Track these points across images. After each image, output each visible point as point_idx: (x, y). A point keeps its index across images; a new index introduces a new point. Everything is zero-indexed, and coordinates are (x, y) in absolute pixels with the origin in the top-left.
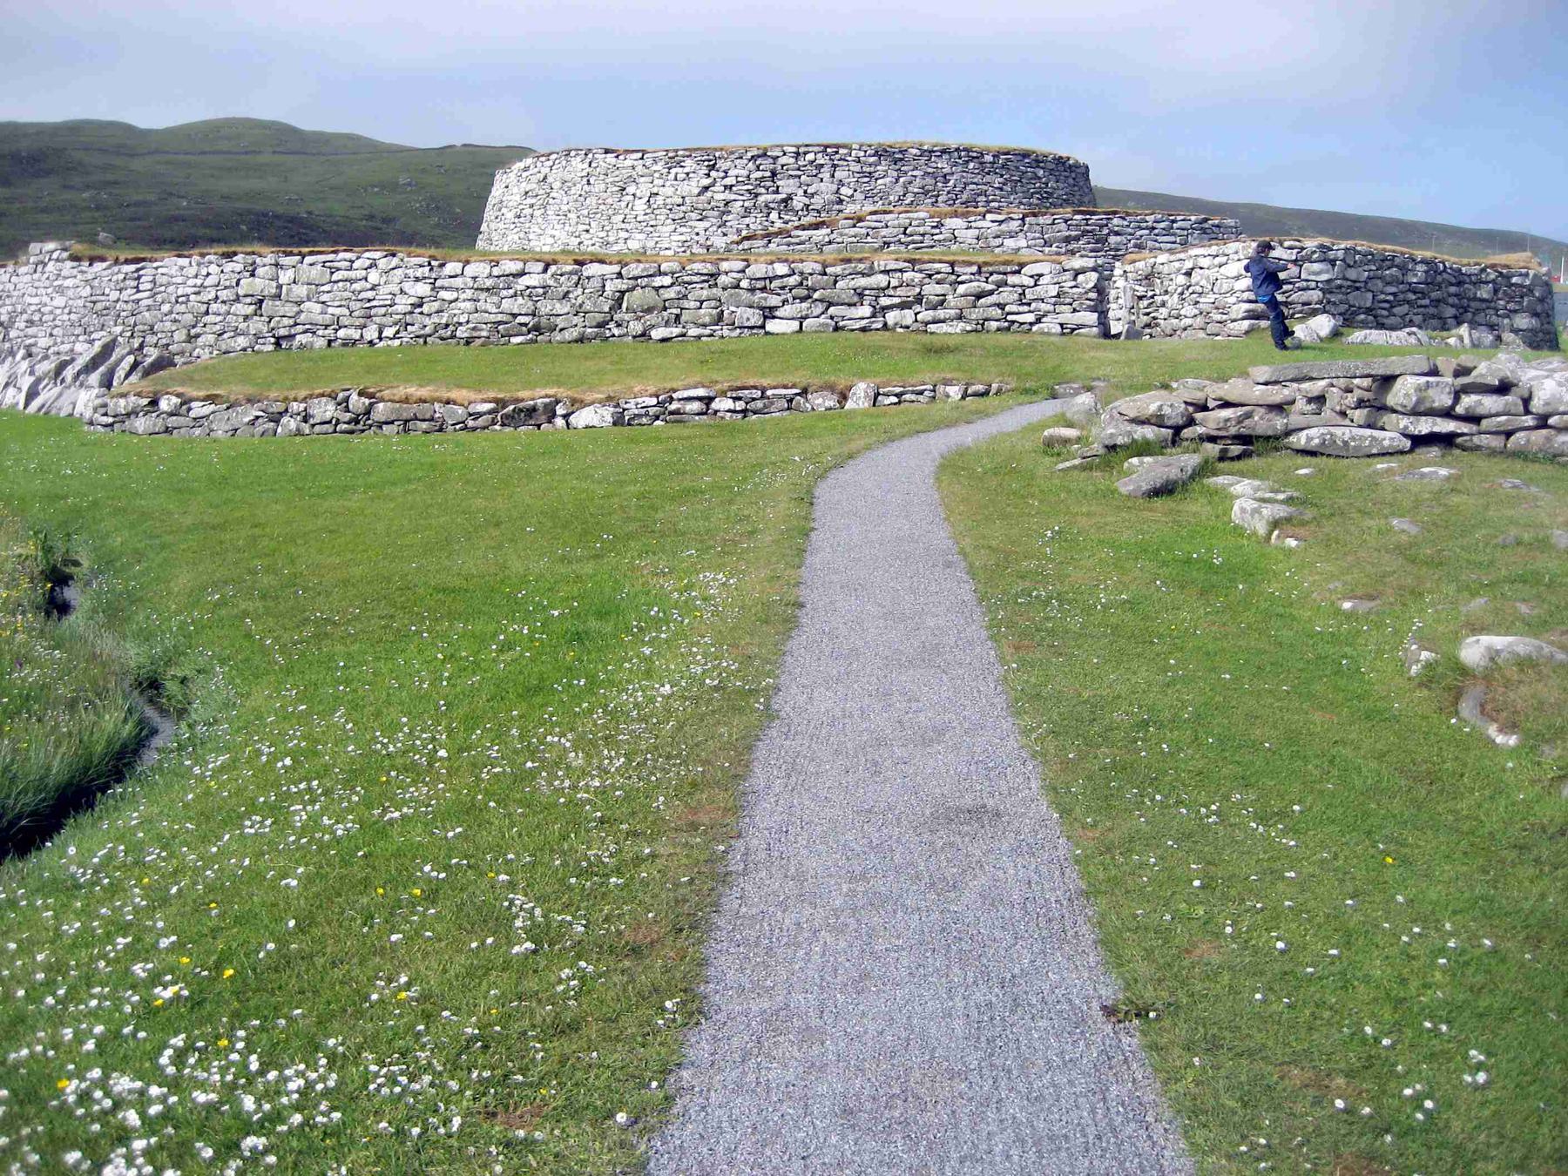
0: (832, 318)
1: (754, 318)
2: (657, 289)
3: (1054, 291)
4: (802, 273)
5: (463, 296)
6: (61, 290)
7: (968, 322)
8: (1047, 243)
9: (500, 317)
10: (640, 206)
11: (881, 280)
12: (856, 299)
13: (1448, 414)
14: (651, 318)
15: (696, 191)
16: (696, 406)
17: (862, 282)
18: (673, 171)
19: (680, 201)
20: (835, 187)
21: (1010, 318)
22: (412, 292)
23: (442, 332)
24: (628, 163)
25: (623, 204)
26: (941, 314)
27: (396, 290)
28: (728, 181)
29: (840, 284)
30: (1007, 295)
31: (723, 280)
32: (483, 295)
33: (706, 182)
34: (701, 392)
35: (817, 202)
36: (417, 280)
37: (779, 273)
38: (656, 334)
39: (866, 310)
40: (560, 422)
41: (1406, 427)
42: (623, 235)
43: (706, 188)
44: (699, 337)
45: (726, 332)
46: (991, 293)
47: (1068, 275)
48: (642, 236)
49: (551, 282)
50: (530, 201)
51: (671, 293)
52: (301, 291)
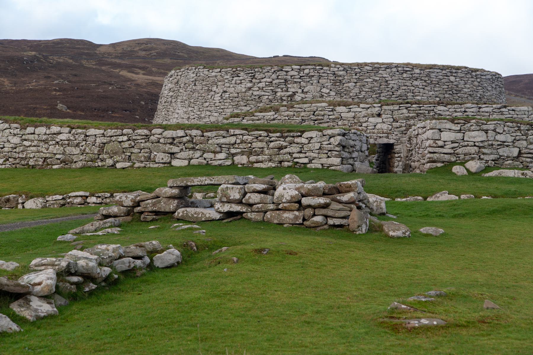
0: (205, 159)
1: (167, 158)
2: (120, 142)
3: (317, 146)
4: (190, 136)
5: (33, 144)
7: (274, 162)
8: (395, 120)
9: (48, 155)
10: (217, 98)
11: (232, 140)
12: (218, 149)
13: (239, 202)
14: (116, 158)
15: (244, 90)
16: (79, 200)
17: (222, 141)
18: (235, 78)
19: (236, 95)
20: (319, 89)
21: (295, 160)
22: (12, 141)
23: (23, 162)
24: (214, 74)
25: (210, 96)
26: (260, 158)
27: (5, 140)
28: (260, 85)
29: (210, 142)
30: (294, 149)
31: (152, 138)
32: (41, 144)
33: (249, 85)
34: (81, 193)
35: (309, 96)
36: (15, 135)
37: (179, 135)
38: (119, 165)
40: (20, 206)
41: (219, 208)
42: (208, 113)
43: (250, 89)
44: (139, 168)
45: (152, 166)
46: (286, 147)
47: (325, 138)
48: (216, 114)
49: (72, 138)
50: (171, 94)
51: (126, 145)
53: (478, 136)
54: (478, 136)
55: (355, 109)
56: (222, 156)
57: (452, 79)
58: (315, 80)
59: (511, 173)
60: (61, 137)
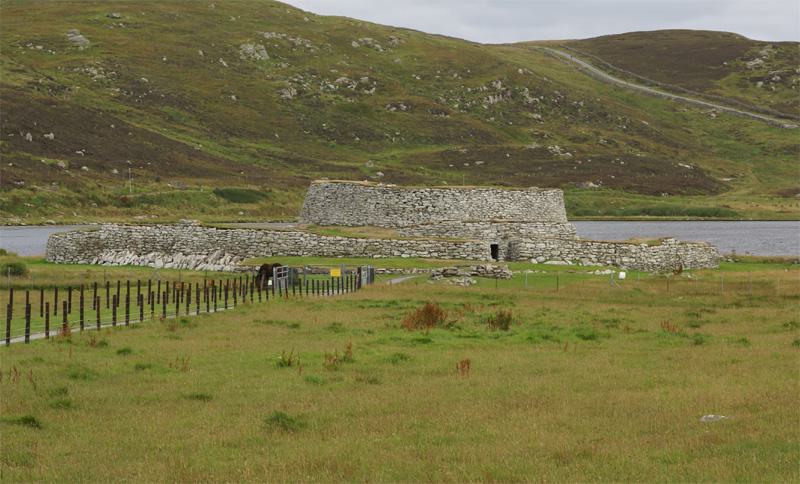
6: (196, 235)
10: (372, 207)
39: (426, 253)
52: (280, 241)
53: (542, 246)
54: (542, 246)
55: (476, 224)
56: (426, 253)
57: (528, 197)
59: (555, 263)
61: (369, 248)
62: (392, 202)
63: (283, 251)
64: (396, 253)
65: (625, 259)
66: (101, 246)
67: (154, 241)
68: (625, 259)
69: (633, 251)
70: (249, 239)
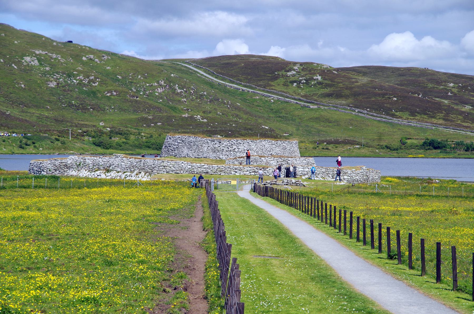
6: (124, 162)
10: (206, 148)
35: (240, 150)
52: (171, 166)
56: (248, 172)
58: (242, 145)
60: (204, 167)
61: (219, 170)
62: (216, 146)
63: (173, 171)
64: (233, 173)
65: (345, 177)
66: (67, 167)
67: (98, 165)
68: (345, 177)
69: (349, 173)
70: (154, 164)
